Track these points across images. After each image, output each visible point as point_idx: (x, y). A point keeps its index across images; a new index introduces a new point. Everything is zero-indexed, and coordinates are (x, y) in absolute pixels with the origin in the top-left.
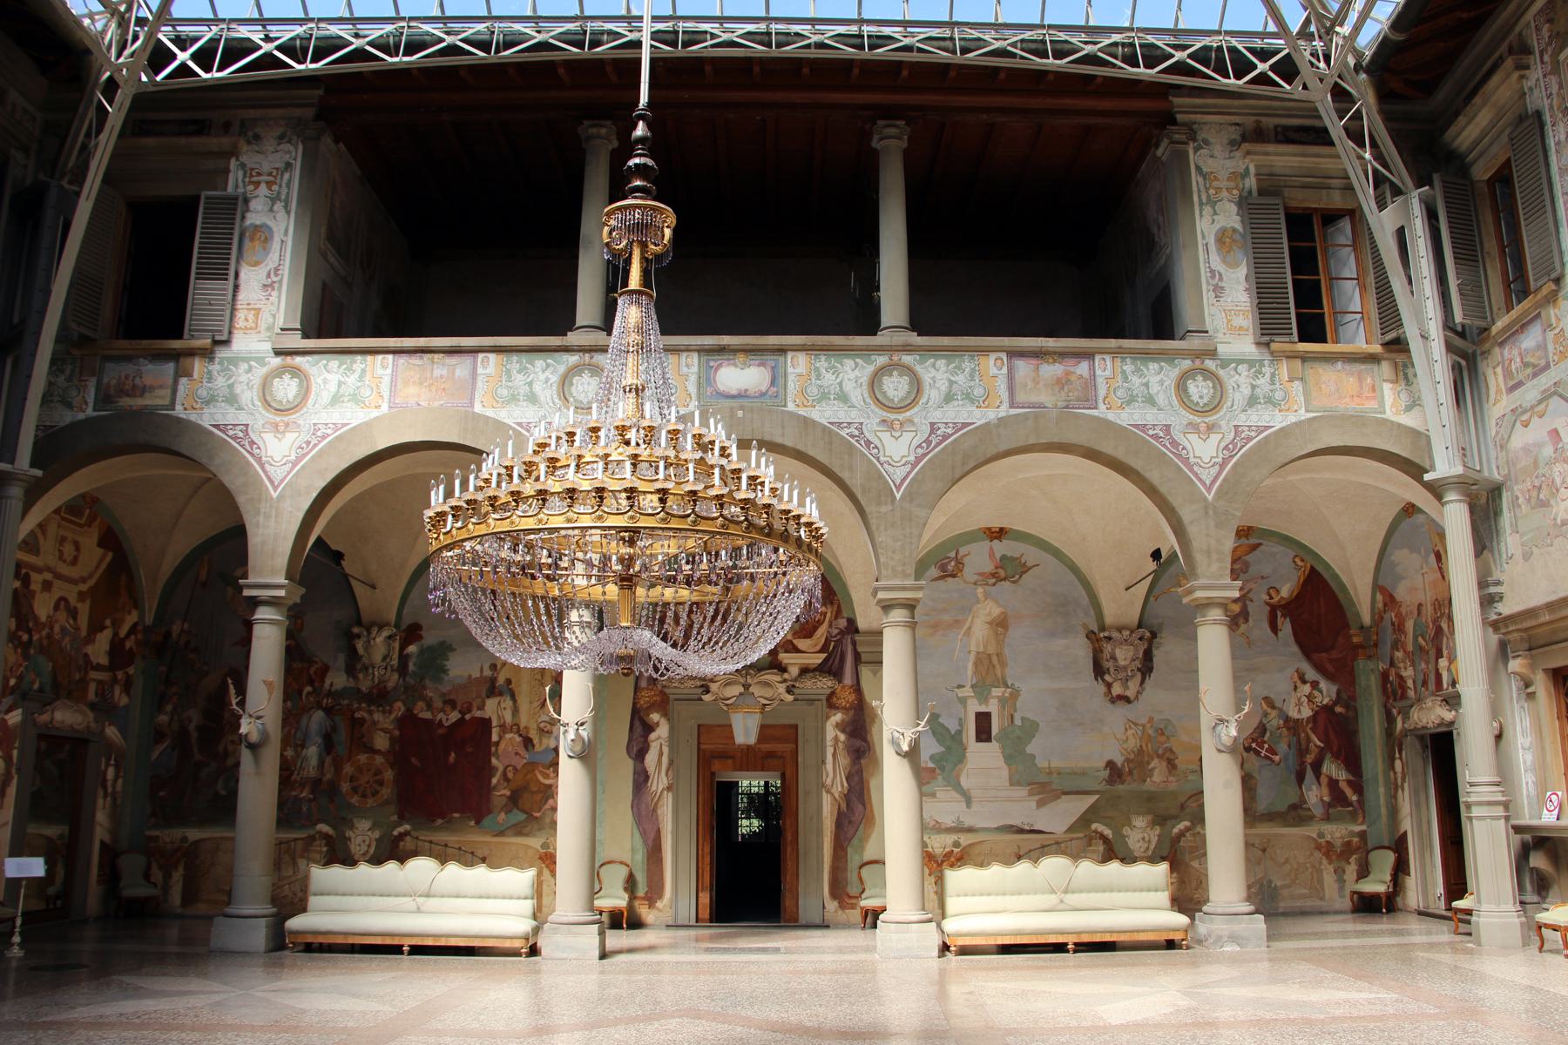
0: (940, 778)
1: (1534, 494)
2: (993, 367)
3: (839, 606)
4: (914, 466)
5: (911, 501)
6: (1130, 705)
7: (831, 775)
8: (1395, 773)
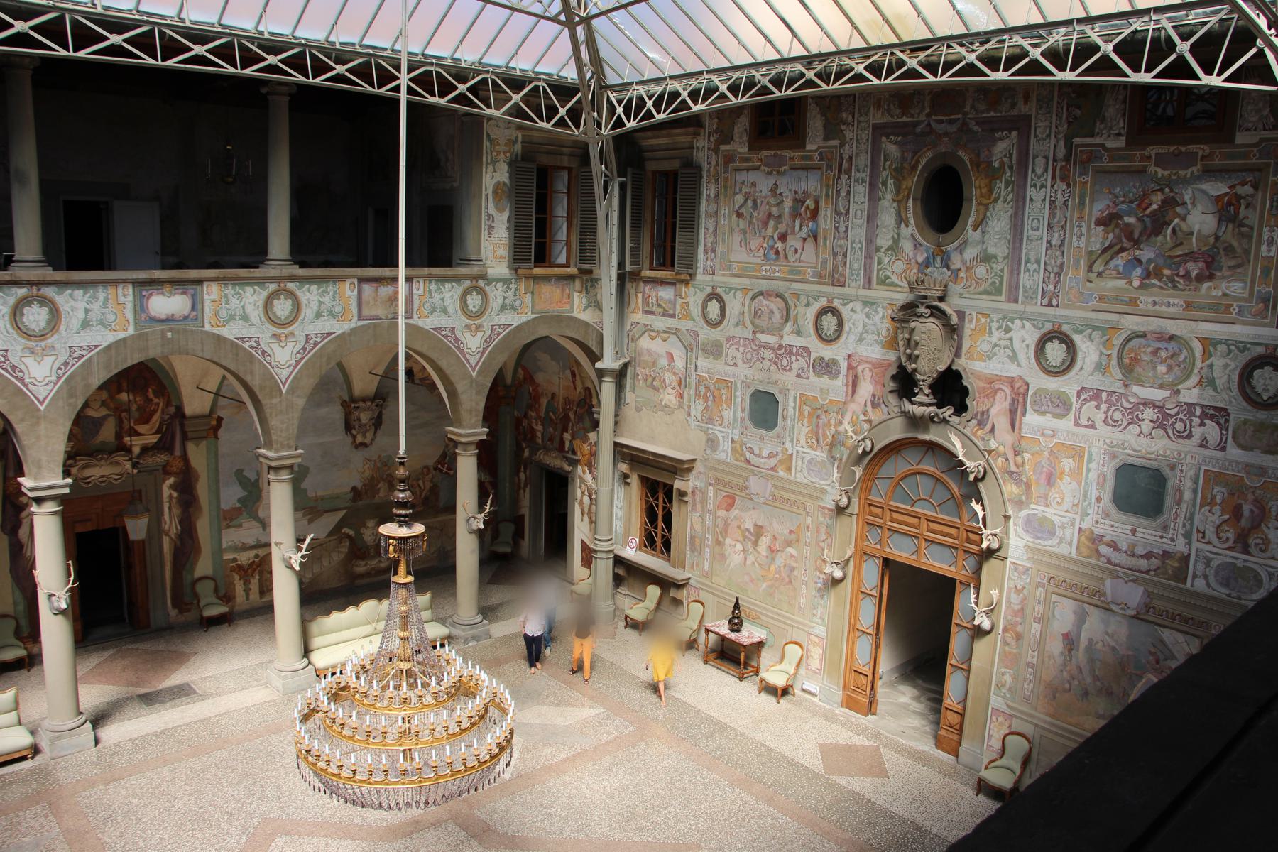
0: (245, 514)
1: (650, 379)
2: (348, 290)
3: (169, 397)
4: (295, 368)
5: (293, 393)
6: (367, 449)
7: (168, 522)
8: (519, 480)
